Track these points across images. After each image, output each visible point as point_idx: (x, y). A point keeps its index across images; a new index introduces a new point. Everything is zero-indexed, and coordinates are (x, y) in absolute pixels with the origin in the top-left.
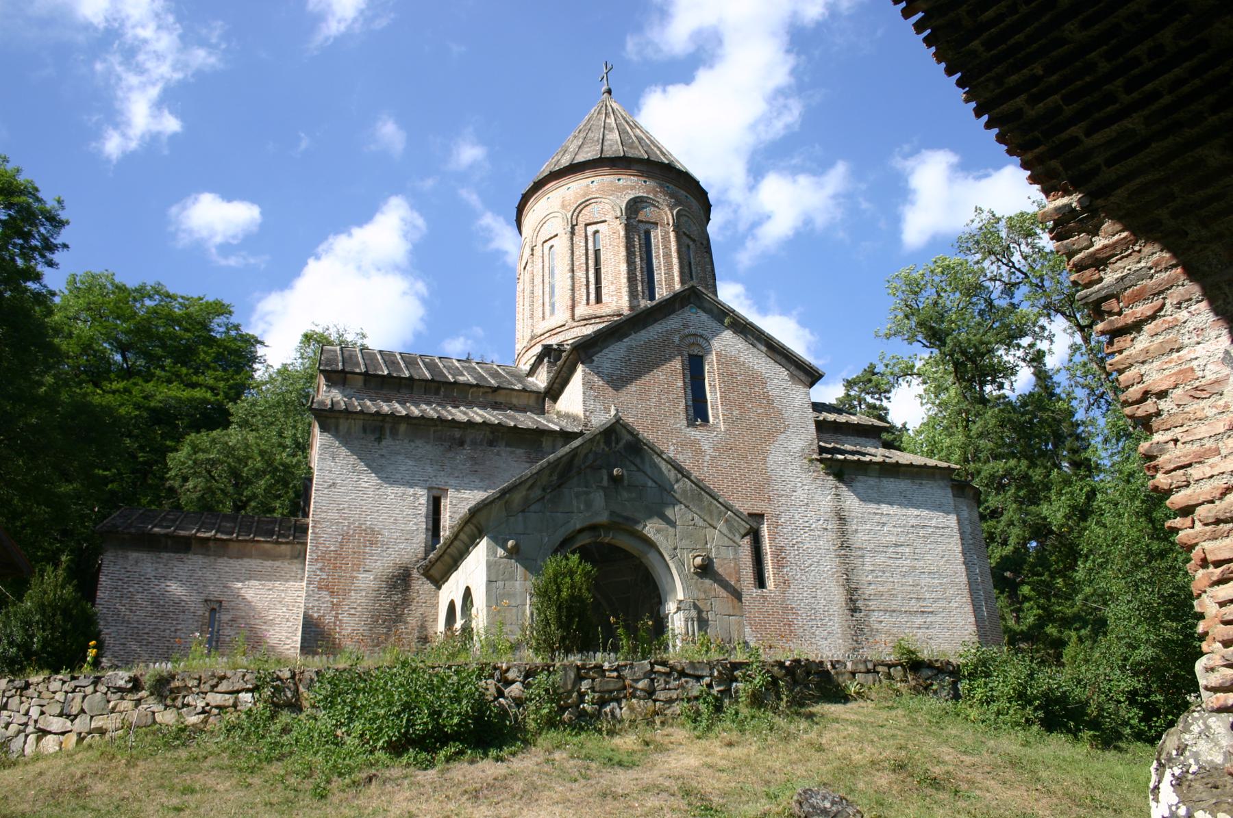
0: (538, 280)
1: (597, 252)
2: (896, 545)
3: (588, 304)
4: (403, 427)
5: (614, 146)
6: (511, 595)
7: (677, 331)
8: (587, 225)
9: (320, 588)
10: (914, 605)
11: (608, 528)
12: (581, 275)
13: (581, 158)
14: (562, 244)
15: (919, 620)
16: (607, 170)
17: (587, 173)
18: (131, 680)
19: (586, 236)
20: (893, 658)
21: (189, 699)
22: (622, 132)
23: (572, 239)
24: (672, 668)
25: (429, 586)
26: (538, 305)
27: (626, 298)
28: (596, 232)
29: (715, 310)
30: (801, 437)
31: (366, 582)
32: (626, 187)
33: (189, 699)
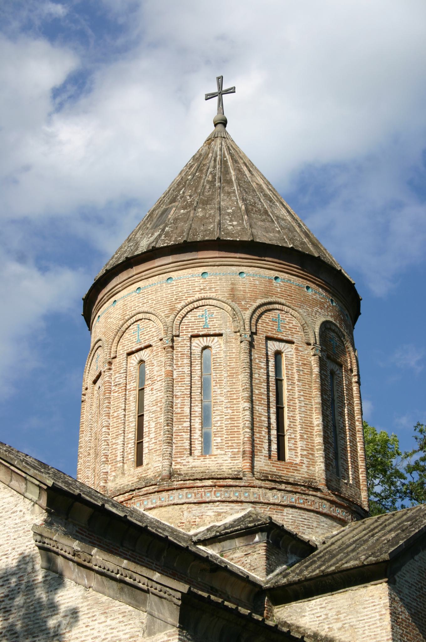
1: (279, 382)
3: (270, 457)
8: (268, 338)
12: (260, 409)
13: (263, 237)
14: (227, 353)
16: (295, 268)
17: (269, 262)
19: (267, 355)
26: (180, 427)
27: (323, 466)
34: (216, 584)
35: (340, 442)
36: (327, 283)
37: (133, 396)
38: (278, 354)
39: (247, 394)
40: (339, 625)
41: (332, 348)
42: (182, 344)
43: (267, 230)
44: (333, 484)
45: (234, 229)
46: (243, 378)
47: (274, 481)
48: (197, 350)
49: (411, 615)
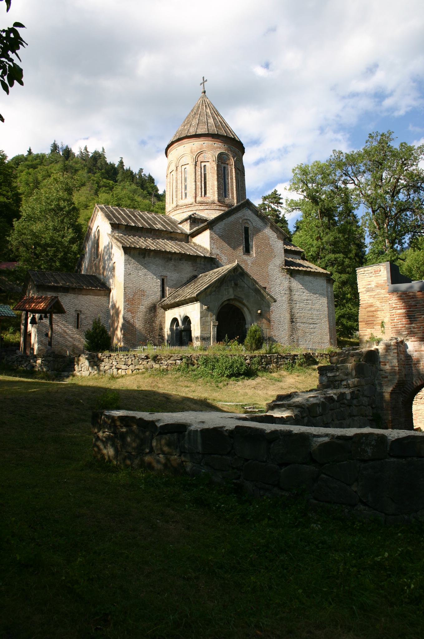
0: (179, 182)
1: (205, 175)
2: (307, 300)
4: (152, 254)
5: (213, 130)
6: (207, 322)
7: (241, 218)
8: (201, 162)
9: (128, 311)
10: (311, 321)
11: (232, 300)
12: (199, 184)
13: (199, 132)
14: (190, 169)
15: (312, 326)
16: (210, 139)
17: (202, 139)
18: (146, 356)
20: (327, 353)
21: (163, 362)
22: (214, 119)
23: (195, 168)
24: (282, 356)
25: (162, 310)
28: (205, 166)
30: (279, 259)
31: (143, 309)
32: (217, 148)
33: (163, 362)
34: (173, 236)
35: (227, 187)
36: (222, 140)
37: (171, 184)
38: (205, 166)
39: (194, 180)
41: (221, 160)
42: (179, 169)
43: (202, 129)
44: (222, 200)
45: (192, 132)
46: (194, 174)
47: (201, 203)
48: (183, 170)
49: (219, 237)
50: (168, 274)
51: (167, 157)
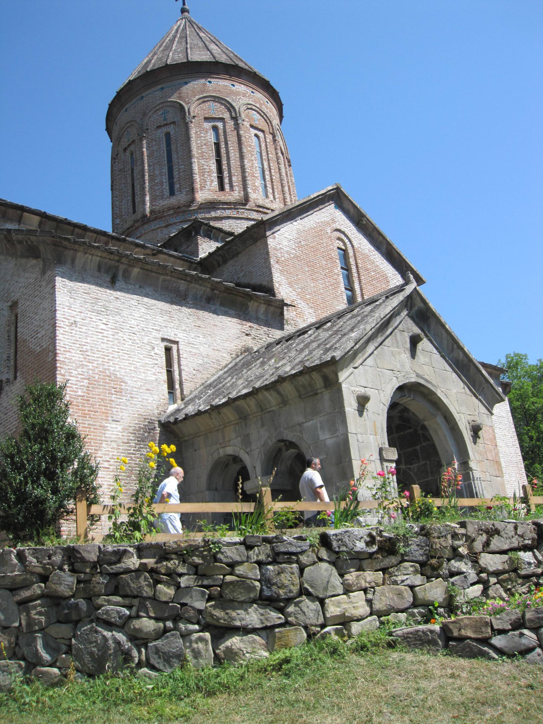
7: (328, 224)
29: (352, 210)
40: (243, 274)
50: (180, 336)
51: (109, 130)
